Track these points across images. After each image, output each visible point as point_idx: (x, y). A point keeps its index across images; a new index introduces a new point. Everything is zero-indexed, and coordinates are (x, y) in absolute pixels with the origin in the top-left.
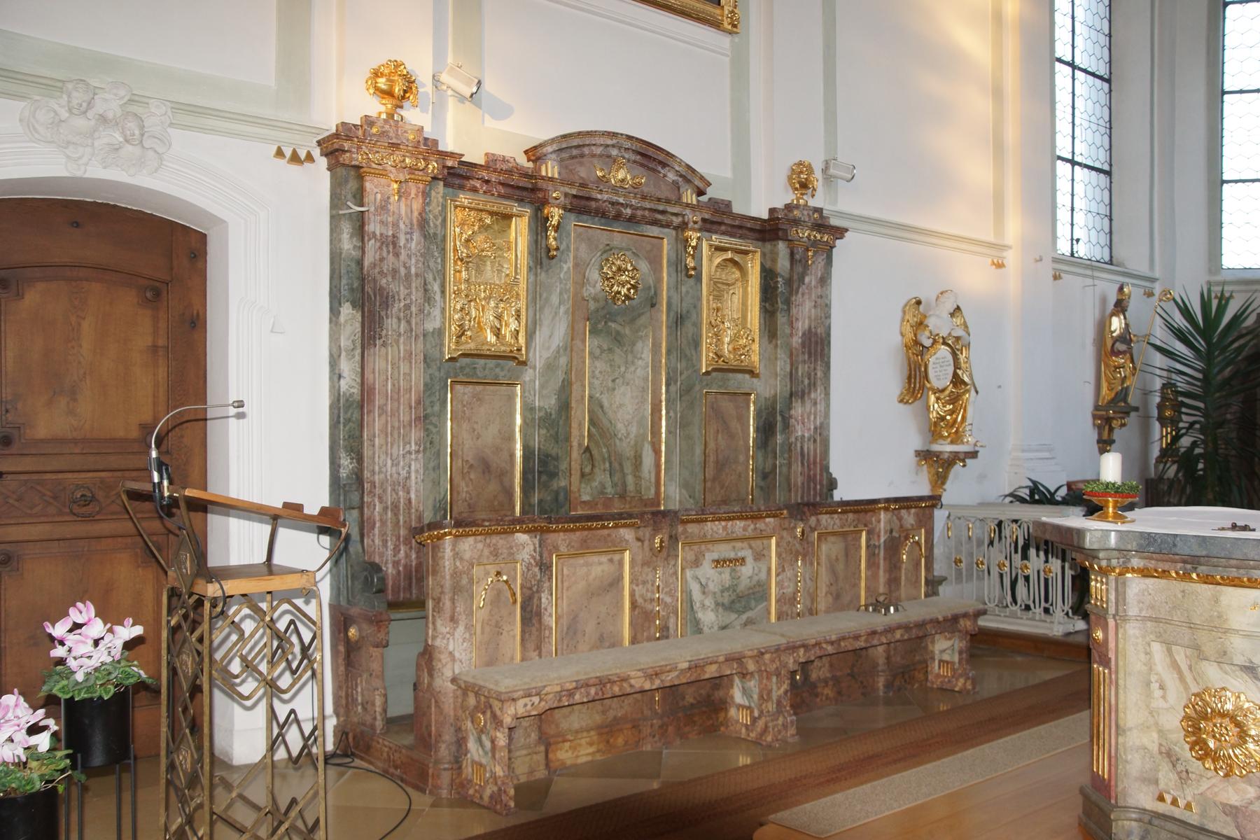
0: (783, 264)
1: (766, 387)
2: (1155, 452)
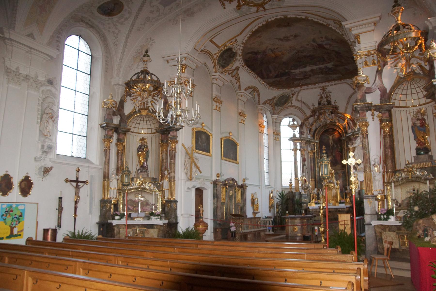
0: (243, 191)
1: (242, 205)
2: (275, 212)
